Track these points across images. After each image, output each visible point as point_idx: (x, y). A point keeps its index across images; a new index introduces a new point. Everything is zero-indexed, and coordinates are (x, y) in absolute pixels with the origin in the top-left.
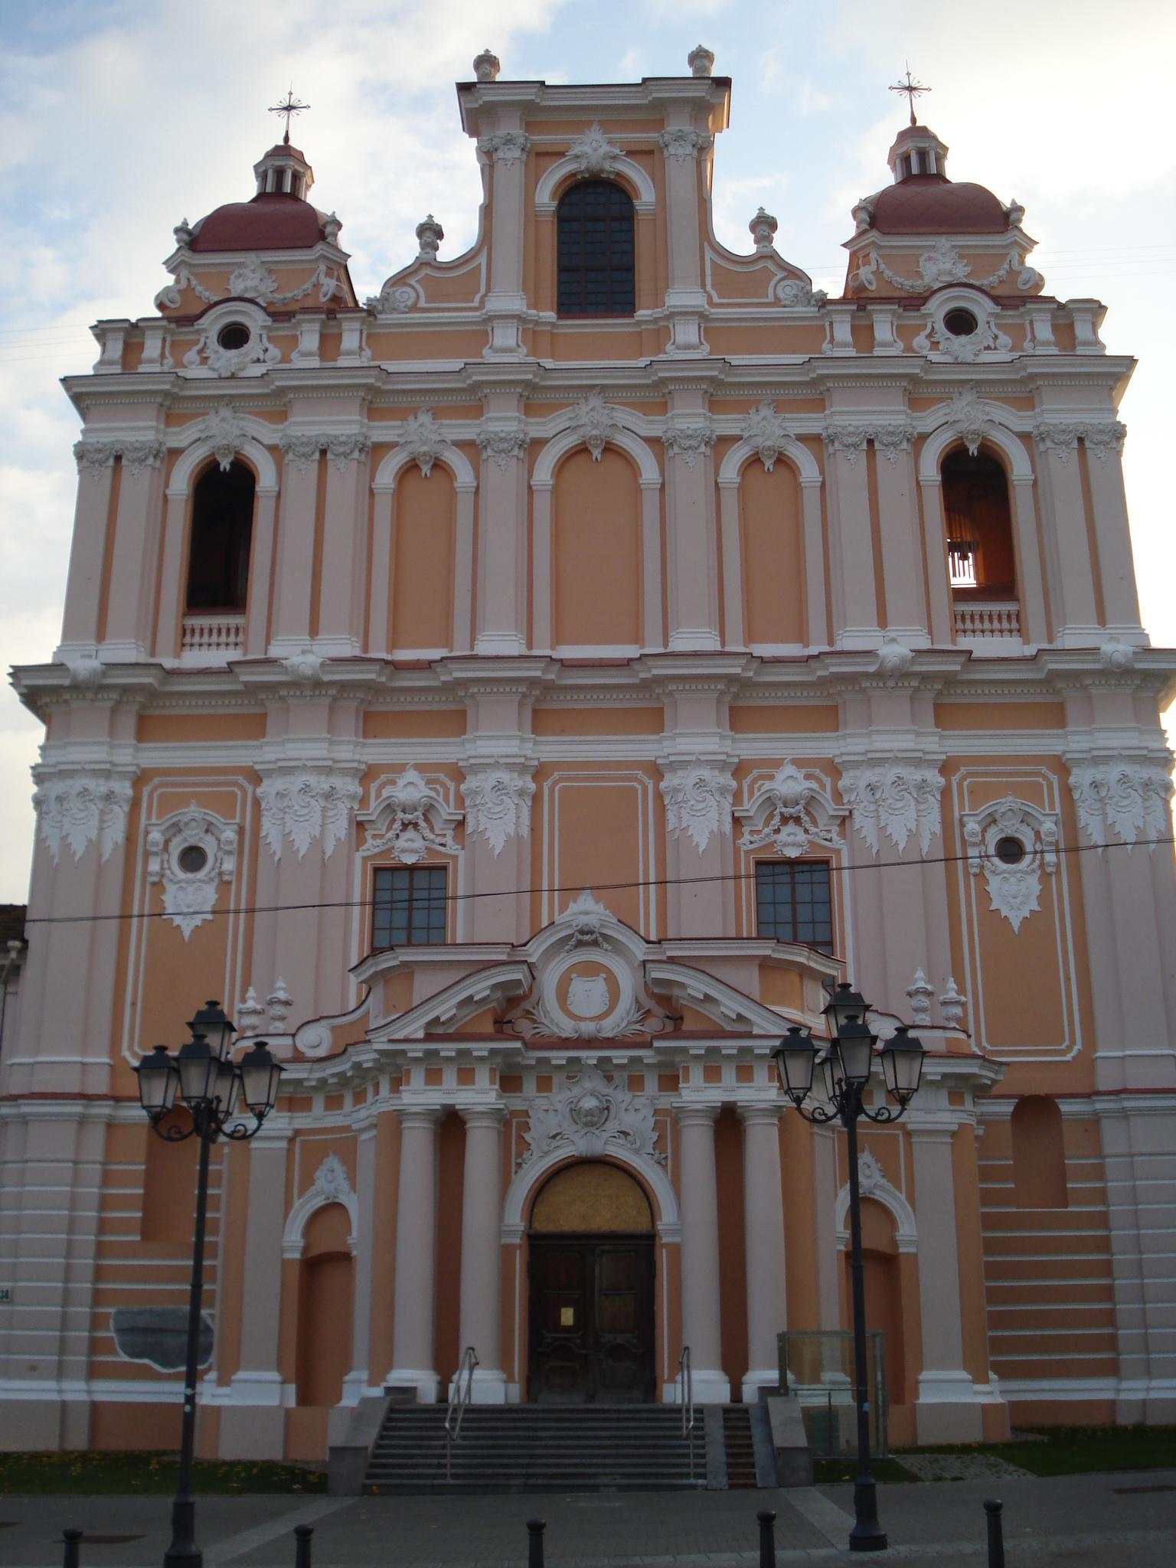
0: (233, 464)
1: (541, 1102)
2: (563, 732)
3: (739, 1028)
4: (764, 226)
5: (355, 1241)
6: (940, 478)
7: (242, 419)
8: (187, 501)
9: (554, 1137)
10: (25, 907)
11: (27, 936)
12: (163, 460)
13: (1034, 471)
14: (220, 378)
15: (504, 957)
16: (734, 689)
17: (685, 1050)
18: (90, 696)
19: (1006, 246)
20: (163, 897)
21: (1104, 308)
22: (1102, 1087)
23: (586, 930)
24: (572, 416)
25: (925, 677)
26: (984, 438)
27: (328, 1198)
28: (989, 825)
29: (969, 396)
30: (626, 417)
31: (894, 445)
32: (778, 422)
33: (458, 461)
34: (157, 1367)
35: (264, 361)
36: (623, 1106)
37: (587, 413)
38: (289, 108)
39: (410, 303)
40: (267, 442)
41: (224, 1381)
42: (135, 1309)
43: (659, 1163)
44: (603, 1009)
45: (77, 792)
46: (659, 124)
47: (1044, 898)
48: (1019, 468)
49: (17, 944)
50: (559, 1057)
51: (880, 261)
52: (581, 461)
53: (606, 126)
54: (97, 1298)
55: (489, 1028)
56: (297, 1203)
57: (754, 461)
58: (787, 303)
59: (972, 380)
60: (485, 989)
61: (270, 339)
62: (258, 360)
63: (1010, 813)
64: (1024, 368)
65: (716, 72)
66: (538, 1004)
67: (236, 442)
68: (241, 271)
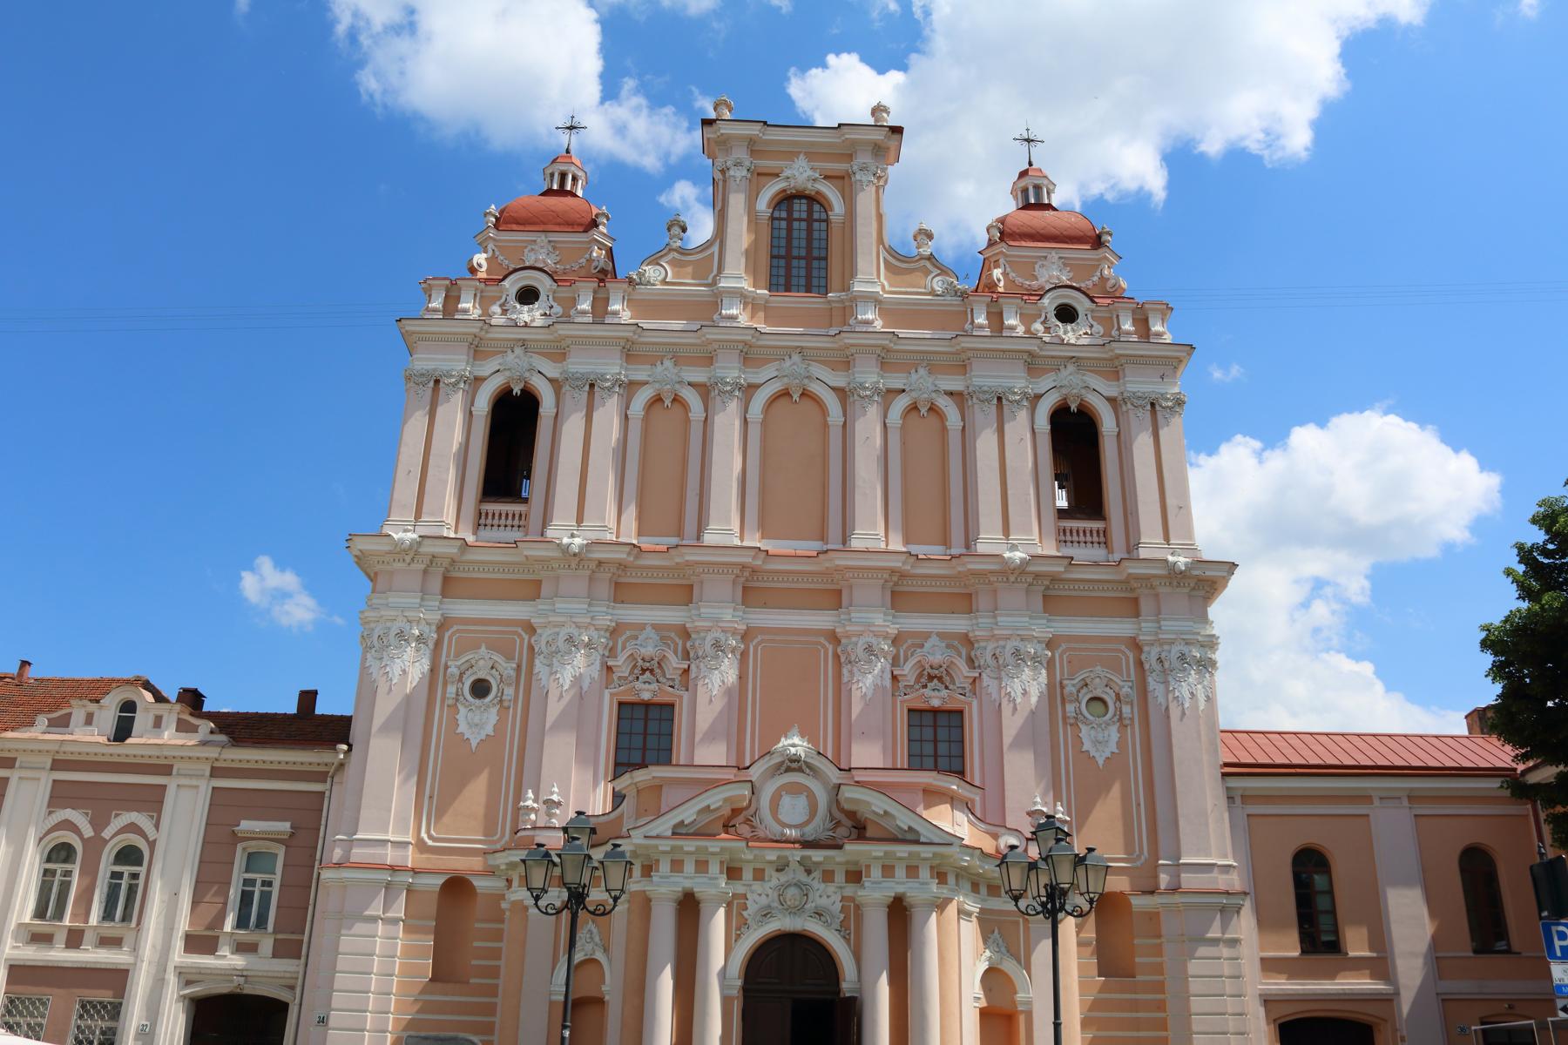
0: (522, 390)
1: (757, 886)
2: (765, 605)
3: (909, 836)
5: (607, 989)
6: (1049, 428)
8: (487, 416)
9: (765, 915)
10: (351, 716)
11: (350, 741)
12: (470, 384)
13: (1118, 425)
14: (517, 326)
15: (731, 777)
19: (1098, 260)
20: (458, 717)
23: (794, 758)
25: (1037, 576)
26: (1082, 400)
27: (586, 955)
28: (1082, 688)
29: (1071, 368)
32: (931, 380)
33: (692, 398)
35: (550, 315)
36: (818, 894)
37: (790, 366)
38: (571, 128)
40: (548, 375)
42: (423, 1034)
43: (844, 937)
44: (804, 818)
45: (396, 633)
46: (850, 157)
47: (1121, 744)
48: (1107, 424)
49: (345, 747)
51: (1007, 266)
52: (784, 401)
53: (812, 154)
57: (914, 408)
59: (1074, 357)
60: (719, 801)
61: (555, 299)
63: (1098, 679)
65: (892, 121)
66: (755, 813)
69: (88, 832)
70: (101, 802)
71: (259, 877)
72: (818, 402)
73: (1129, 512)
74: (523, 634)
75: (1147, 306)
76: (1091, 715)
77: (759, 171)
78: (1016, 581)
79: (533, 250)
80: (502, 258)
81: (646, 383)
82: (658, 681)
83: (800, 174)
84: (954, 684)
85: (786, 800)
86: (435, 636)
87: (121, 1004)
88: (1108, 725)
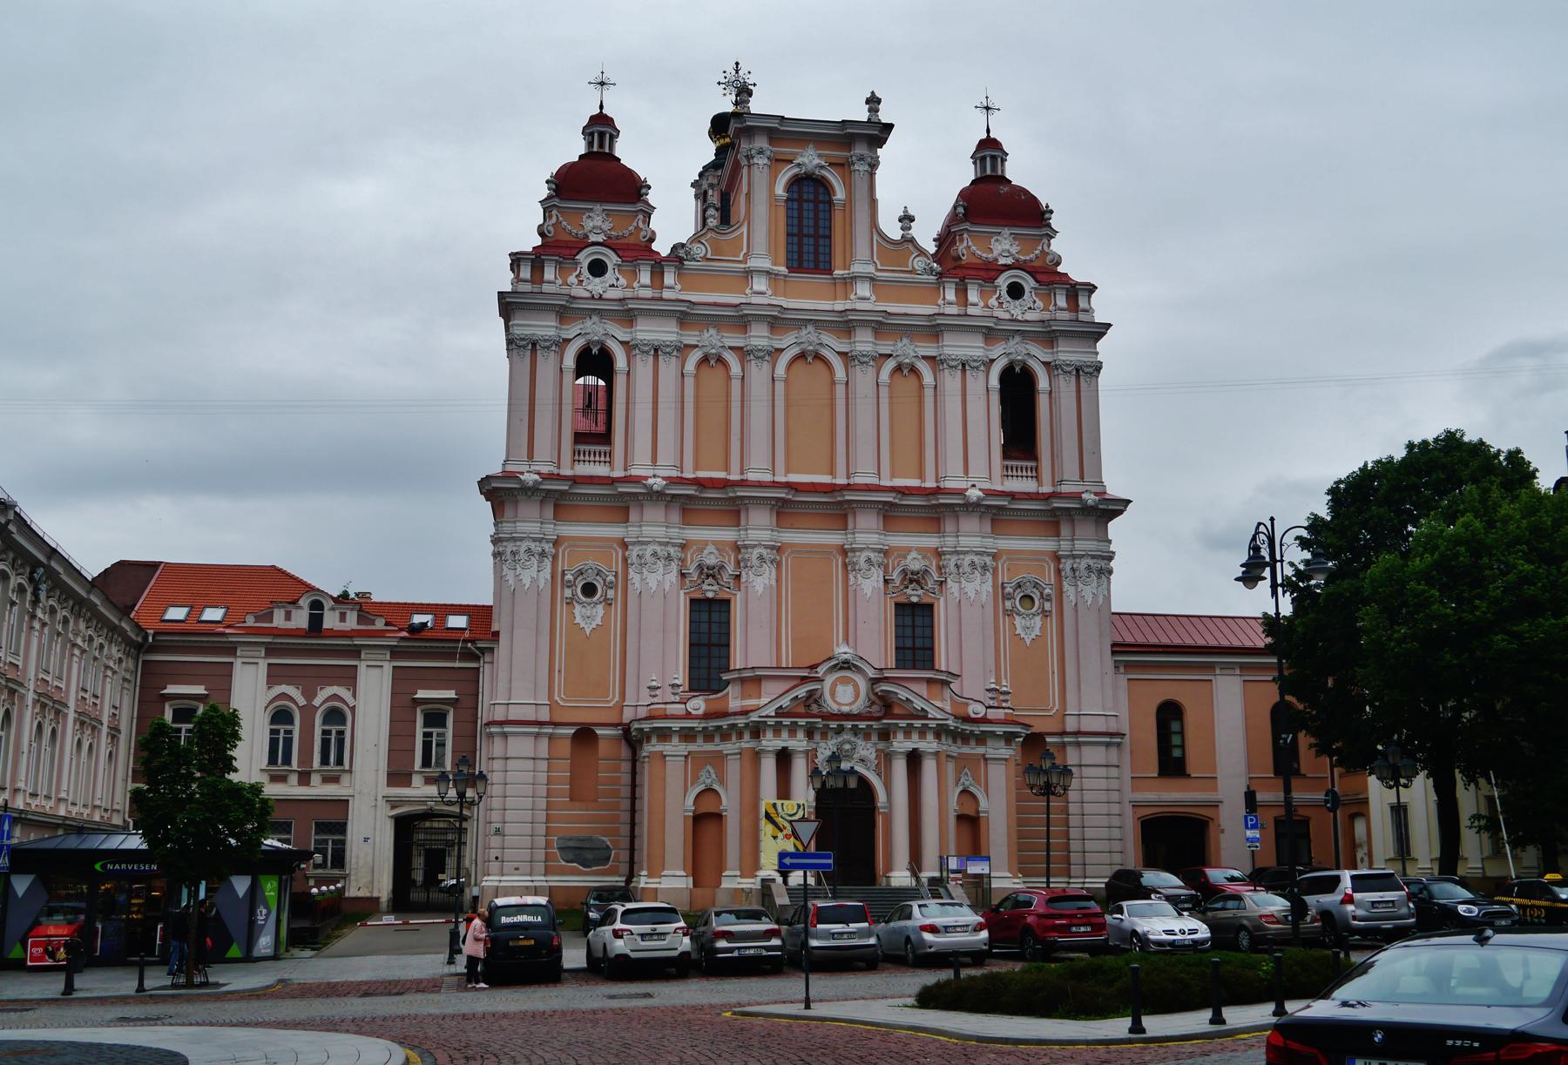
0: (599, 350)
1: (823, 744)
4: (907, 219)
7: (605, 323)
16: (886, 508)
17: (897, 724)
18: (529, 493)
21: (1097, 288)
22: (1068, 729)
24: (797, 335)
28: (1016, 589)
29: (1017, 339)
30: (827, 338)
31: (977, 368)
33: (731, 358)
34: (581, 867)
39: (701, 255)
41: (649, 876)
43: (878, 774)
48: (1043, 383)
50: (833, 725)
54: (548, 832)
55: (802, 710)
56: (690, 790)
57: (899, 368)
58: (919, 272)
62: (613, 285)
64: (1050, 326)
65: (884, 117)
67: (603, 338)
68: (591, 214)
69: (302, 701)
70: (310, 680)
71: (435, 731)
72: (827, 365)
73: (1055, 454)
74: (618, 548)
75: (1078, 287)
76: (1022, 607)
77: (777, 157)
78: (973, 511)
79: (590, 217)
80: (564, 223)
81: (697, 346)
82: (718, 584)
83: (810, 159)
84: (927, 586)
85: (840, 688)
86: (554, 551)
87: (345, 824)
88: (1034, 615)
